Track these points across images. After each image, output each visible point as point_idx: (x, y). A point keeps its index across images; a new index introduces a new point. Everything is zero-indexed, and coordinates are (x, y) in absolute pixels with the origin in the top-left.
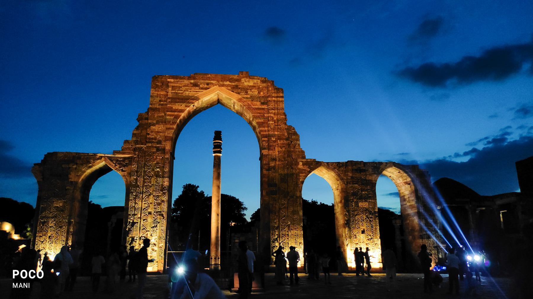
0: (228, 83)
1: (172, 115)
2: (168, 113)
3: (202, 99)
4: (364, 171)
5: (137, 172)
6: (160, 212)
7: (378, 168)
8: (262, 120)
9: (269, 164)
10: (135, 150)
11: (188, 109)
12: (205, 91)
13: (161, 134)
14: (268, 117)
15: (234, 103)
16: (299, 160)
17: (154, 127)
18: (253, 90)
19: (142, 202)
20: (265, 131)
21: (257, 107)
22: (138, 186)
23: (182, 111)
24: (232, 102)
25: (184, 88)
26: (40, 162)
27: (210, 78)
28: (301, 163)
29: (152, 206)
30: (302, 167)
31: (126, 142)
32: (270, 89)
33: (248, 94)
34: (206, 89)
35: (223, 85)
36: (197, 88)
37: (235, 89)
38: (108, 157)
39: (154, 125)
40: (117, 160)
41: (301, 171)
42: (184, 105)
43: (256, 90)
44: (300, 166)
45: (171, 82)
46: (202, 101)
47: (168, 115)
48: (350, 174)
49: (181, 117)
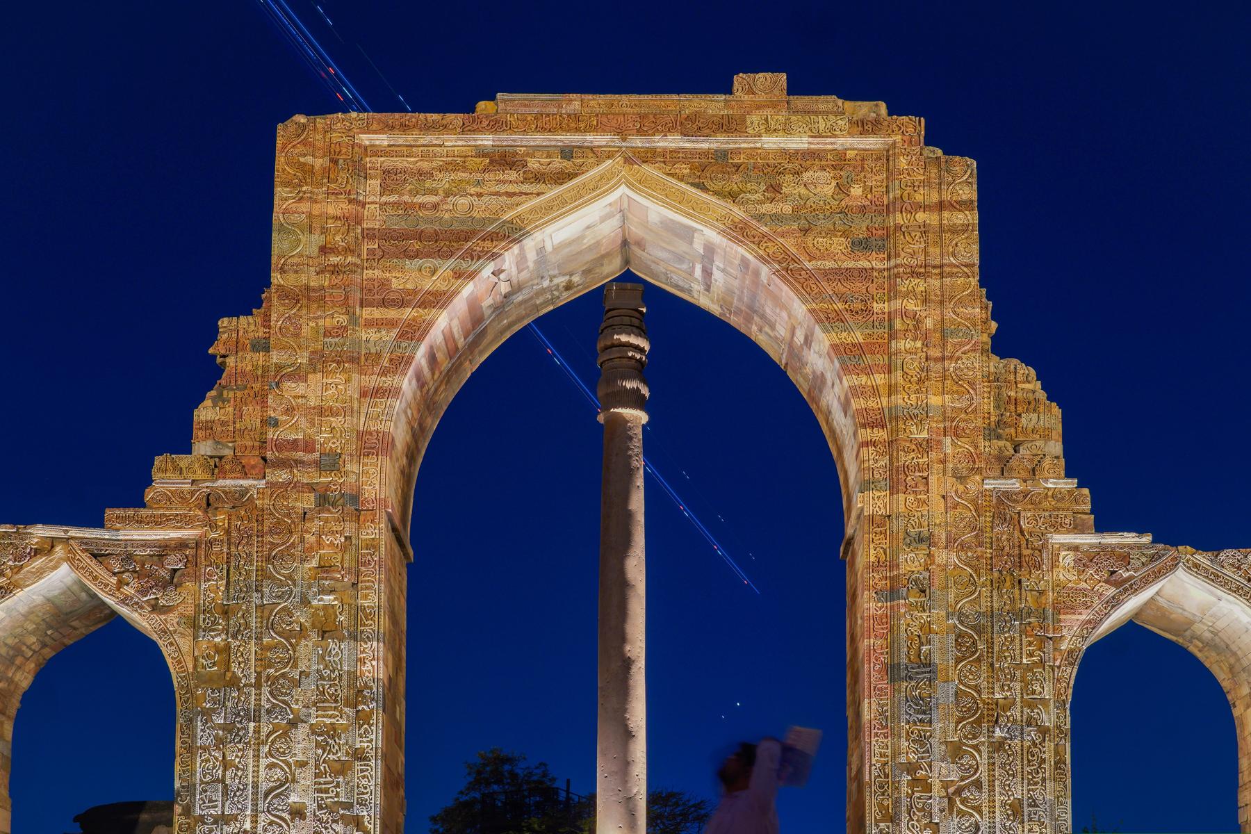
0: (673, 141)
1: (391, 324)
3: (538, 236)
5: (226, 612)
6: (349, 806)
9: (893, 565)
10: (209, 503)
11: (468, 290)
12: (554, 191)
13: (336, 421)
14: (891, 317)
15: (710, 250)
16: (1059, 539)
17: (301, 388)
18: (807, 176)
19: (257, 757)
20: (875, 391)
21: (829, 264)
22: (234, 683)
23: (438, 300)
24: (698, 247)
25: (444, 181)
27: (576, 117)
29: (306, 778)
32: (903, 162)
34: (561, 177)
35: (648, 156)
36: (512, 175)
37: (708, 172)
38: (83, 541)
39: (298, 375)
40: (129, 557)
42: (446, 267)
45: (375, 151)
46: (541, 251)
47: (370, 324)
49: (436, 335)
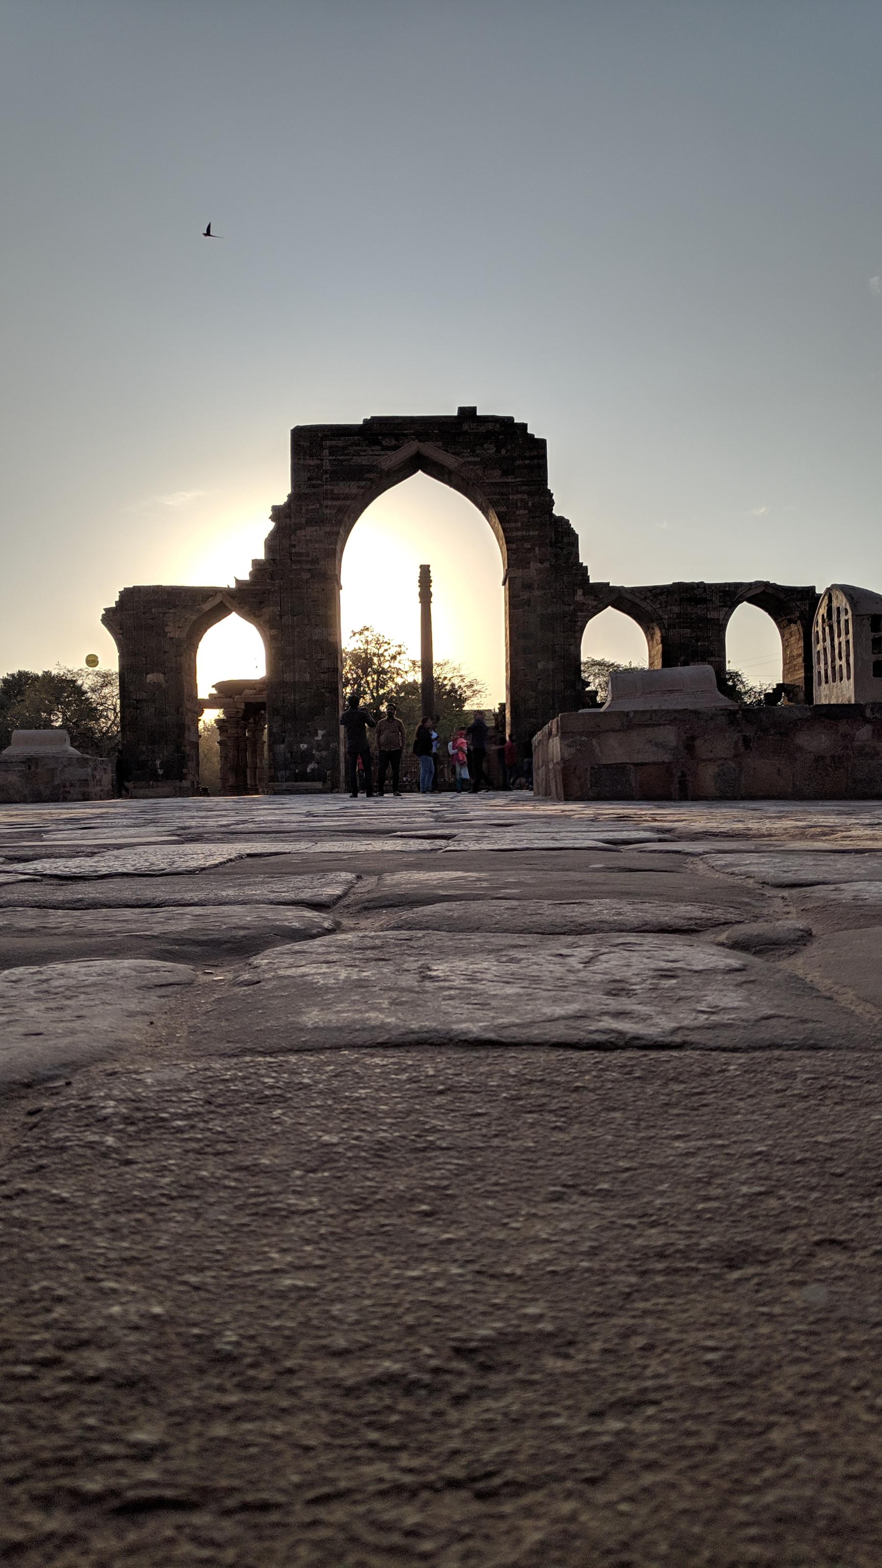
2: (325, 503)
4: (704, 601)
7: (730, 595)
8: (503, 509)
17: (303, 533)
26: (114, 605)
28: (580, 592)
30: (582, 598)
31: (255, 563)
33: (477, 456)
34: (395, 448)
36: (378, 447)
41: (581, 607)
43: (492, 446)
44: (579, 596)
47: (327, 507)
48: (676, 609)
